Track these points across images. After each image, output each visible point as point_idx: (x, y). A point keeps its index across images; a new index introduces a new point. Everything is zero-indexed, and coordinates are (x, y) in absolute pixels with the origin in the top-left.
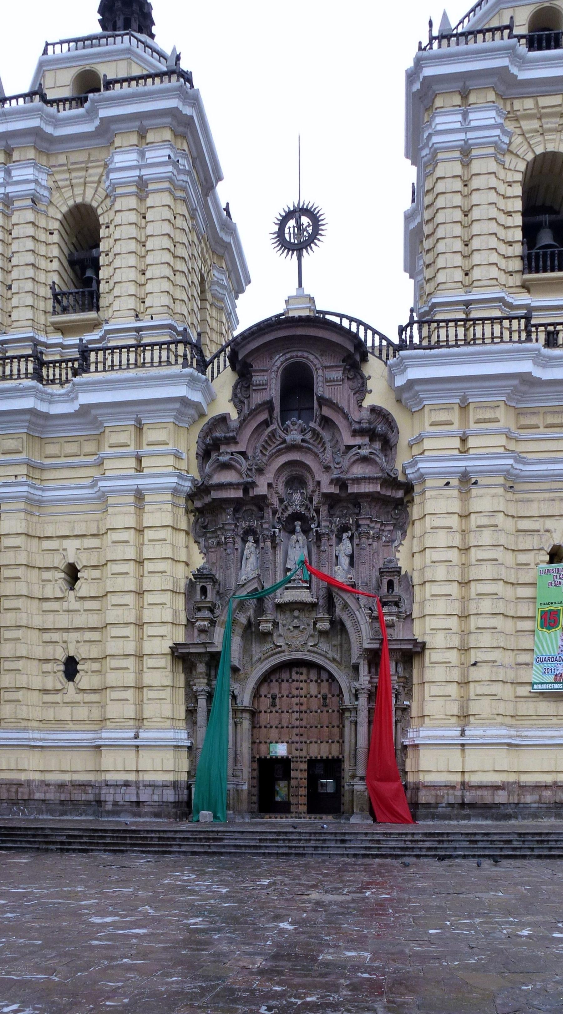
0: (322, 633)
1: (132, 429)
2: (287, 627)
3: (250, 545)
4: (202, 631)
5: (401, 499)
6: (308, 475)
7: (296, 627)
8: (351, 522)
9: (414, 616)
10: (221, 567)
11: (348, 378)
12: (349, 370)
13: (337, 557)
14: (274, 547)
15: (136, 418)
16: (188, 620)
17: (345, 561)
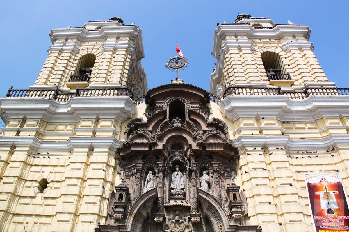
1: (94, 120)
2: (171, 221)
3: (150, 175)
4: (117, 220)
5: (234, 156)
6: (184, 142)
8: (208, 165)
9: (249, 215)
10: (132, 186)
11: (201, 108)
12: (201, 105)
13: (200, 183)
15: (97, 116)
16: (108, 213)
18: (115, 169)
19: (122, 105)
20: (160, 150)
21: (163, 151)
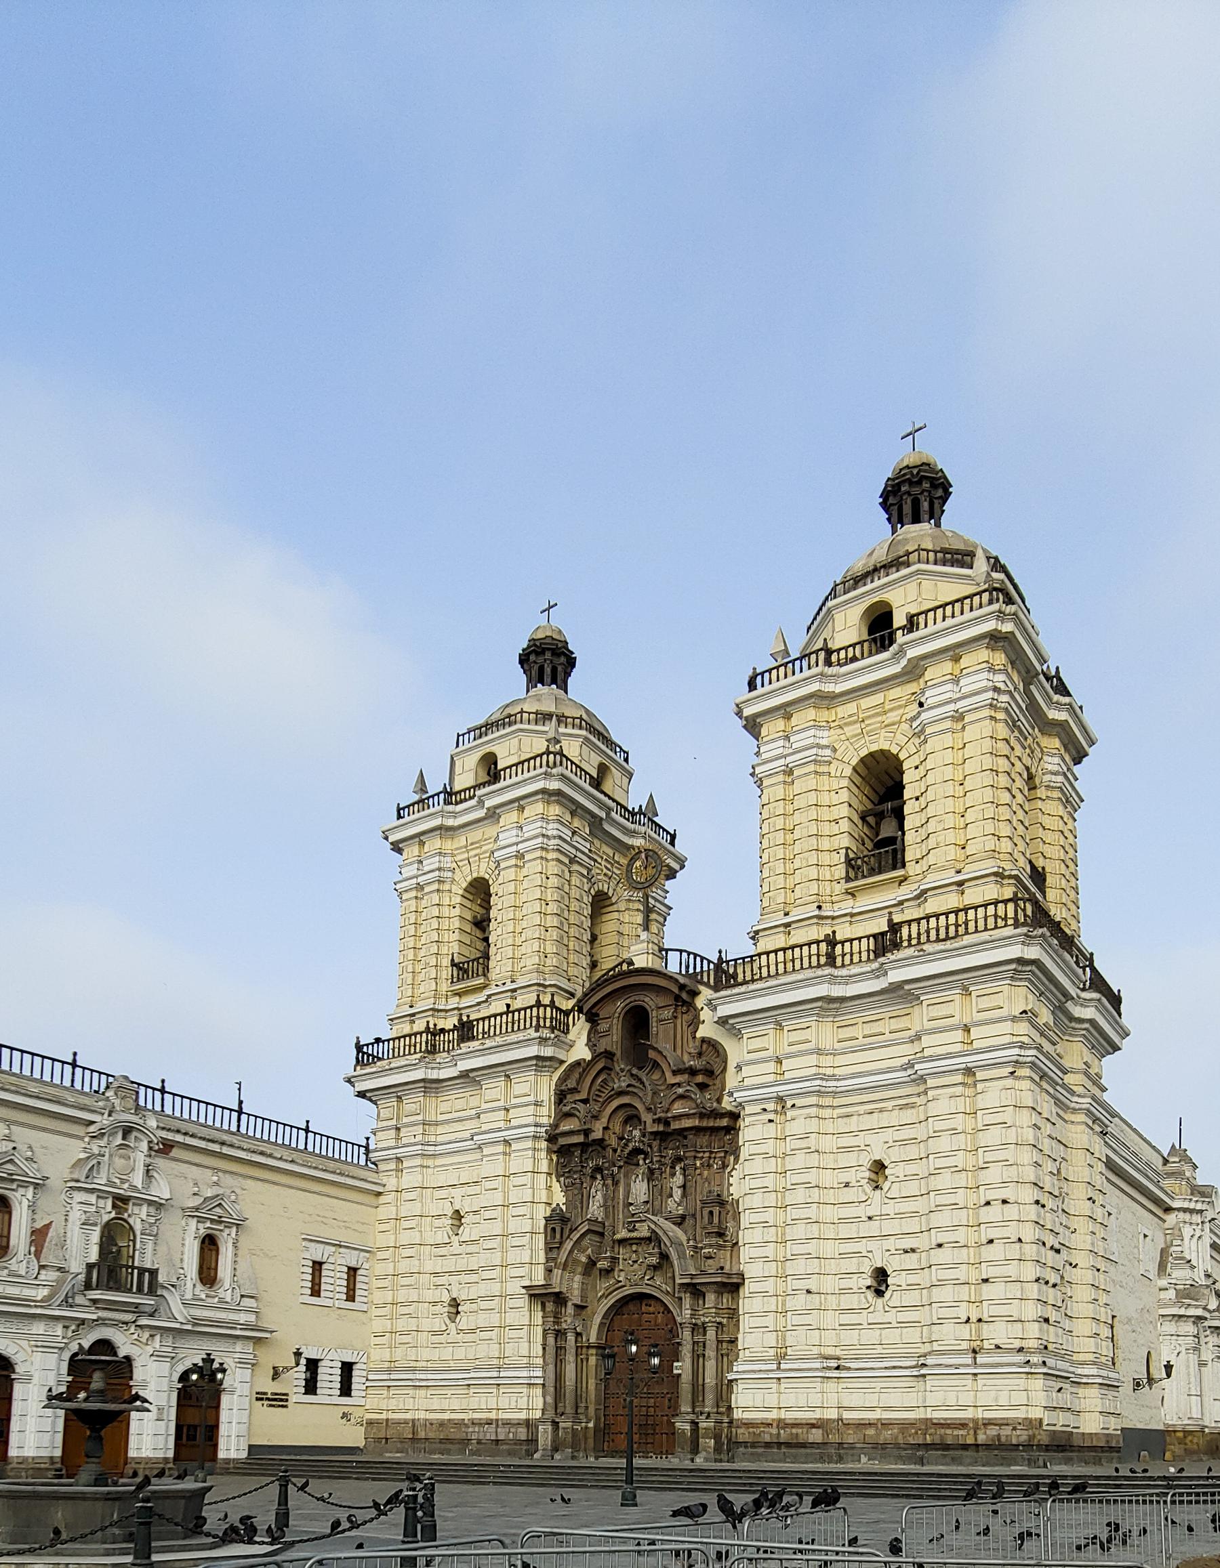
0: (655, 1268)
3: (598, 1183)
7: (635, 1262)
14: (616, 1183)
17: (678, 1193)
18: (549, 1174)
19: (533, 1051)
20: (603, 1140)
21: (607, 1138)
